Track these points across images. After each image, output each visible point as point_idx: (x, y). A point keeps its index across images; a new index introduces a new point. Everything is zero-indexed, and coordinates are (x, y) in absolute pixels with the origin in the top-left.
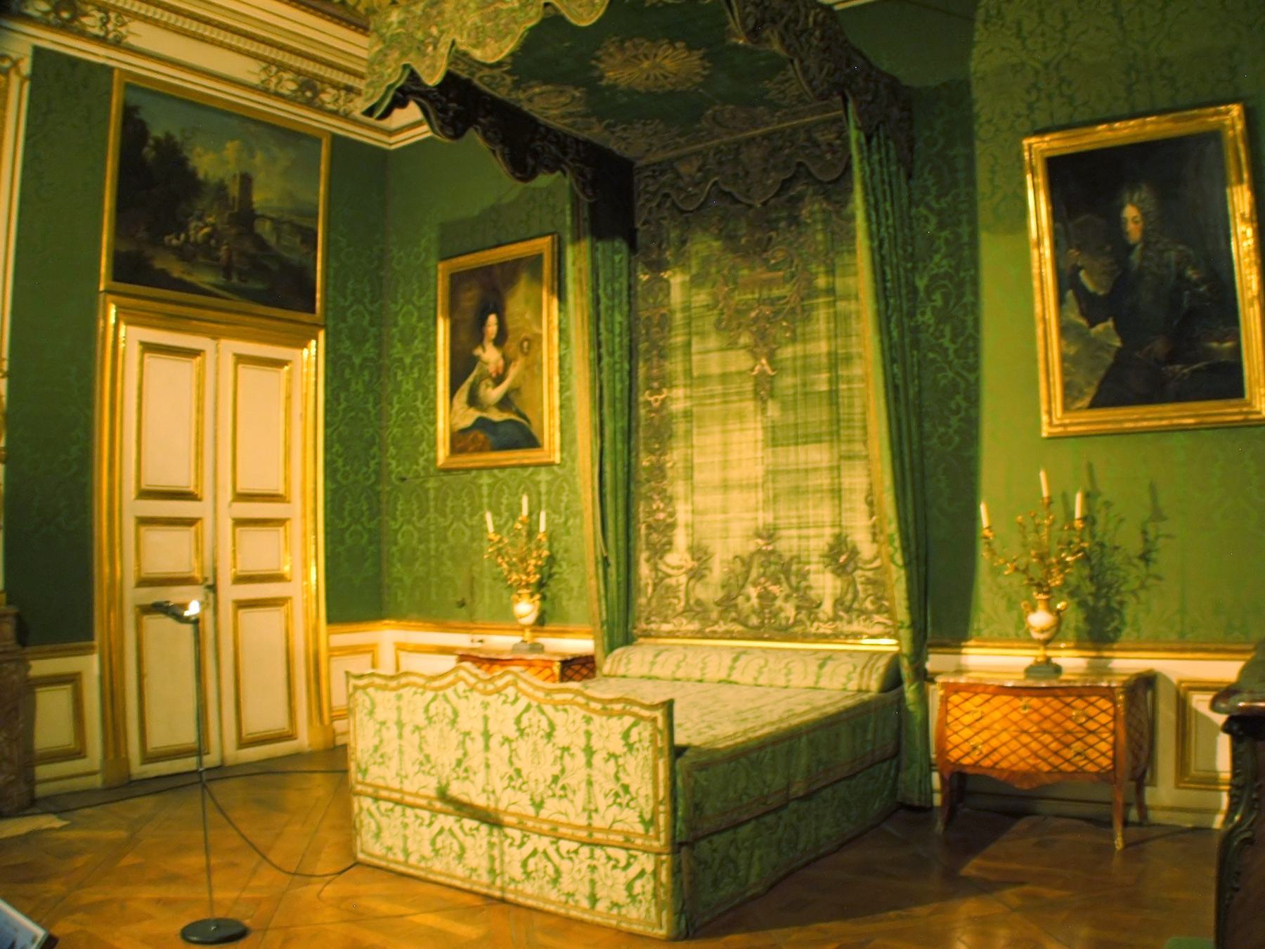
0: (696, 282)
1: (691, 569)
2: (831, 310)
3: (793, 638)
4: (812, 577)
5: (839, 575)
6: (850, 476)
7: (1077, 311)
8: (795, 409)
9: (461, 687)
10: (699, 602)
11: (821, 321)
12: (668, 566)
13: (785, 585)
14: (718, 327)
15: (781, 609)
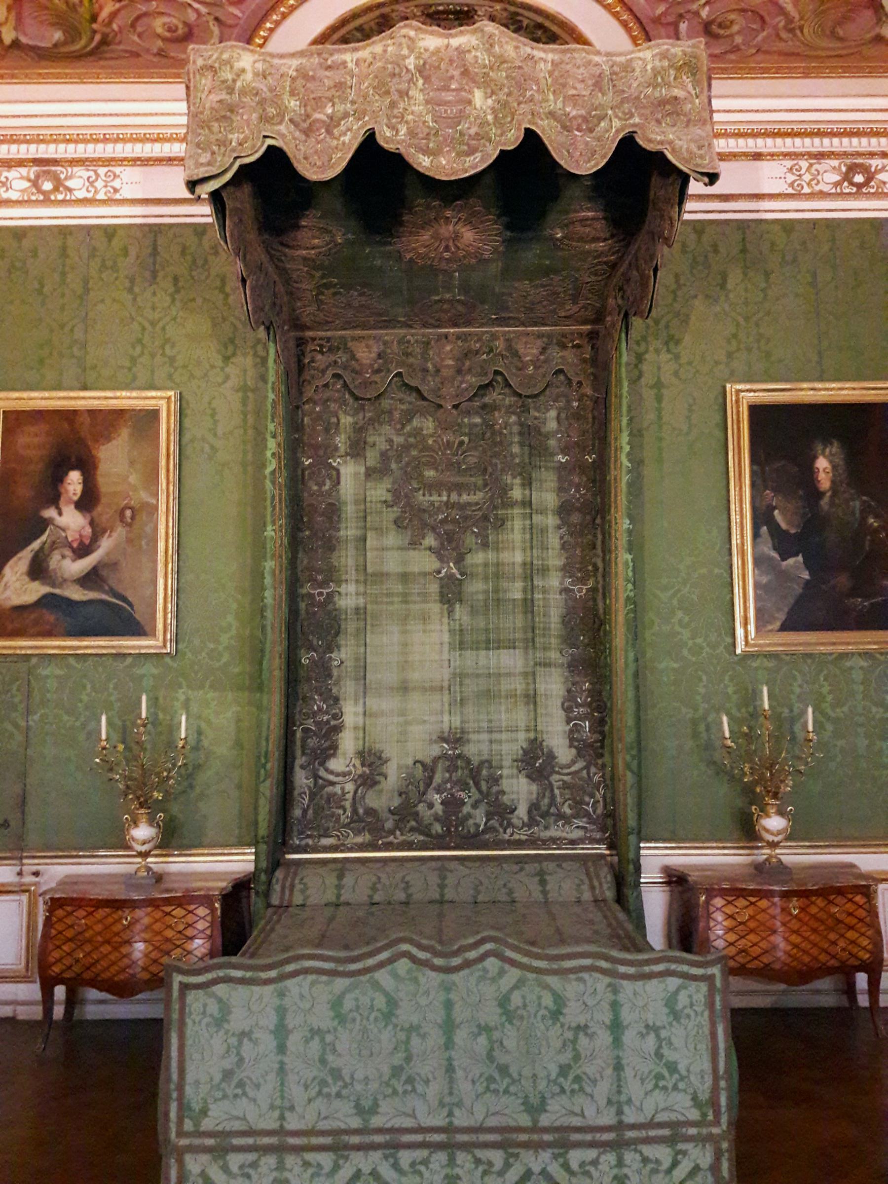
1: (360, 776)
5: (533, 780)
7: (770, 545)
8: (486, 613)
9: (403, 965)
10: (371, 812)
13: (473, 790)
15: (469, 816)
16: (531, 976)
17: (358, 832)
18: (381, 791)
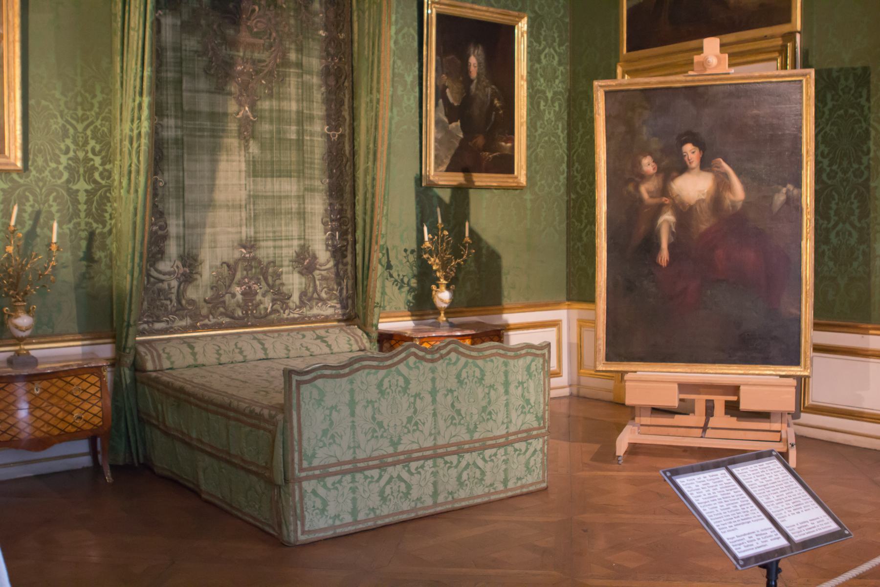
0: (187, 28)
1: (182, 274)
2: (300, 80)
3: (271, 324)
4: (284, 276)
6: (312, 204)
7: (443, 113)
8: (271, 150)
9: (412, 359)
10: (192, 302)
11: (292, 86)
12: (160, 272)
13: (263, 283)
14: (207, 71)
15: (261, 302)
16: (470, 361)
17: (182, 318)
18: (198, 286)
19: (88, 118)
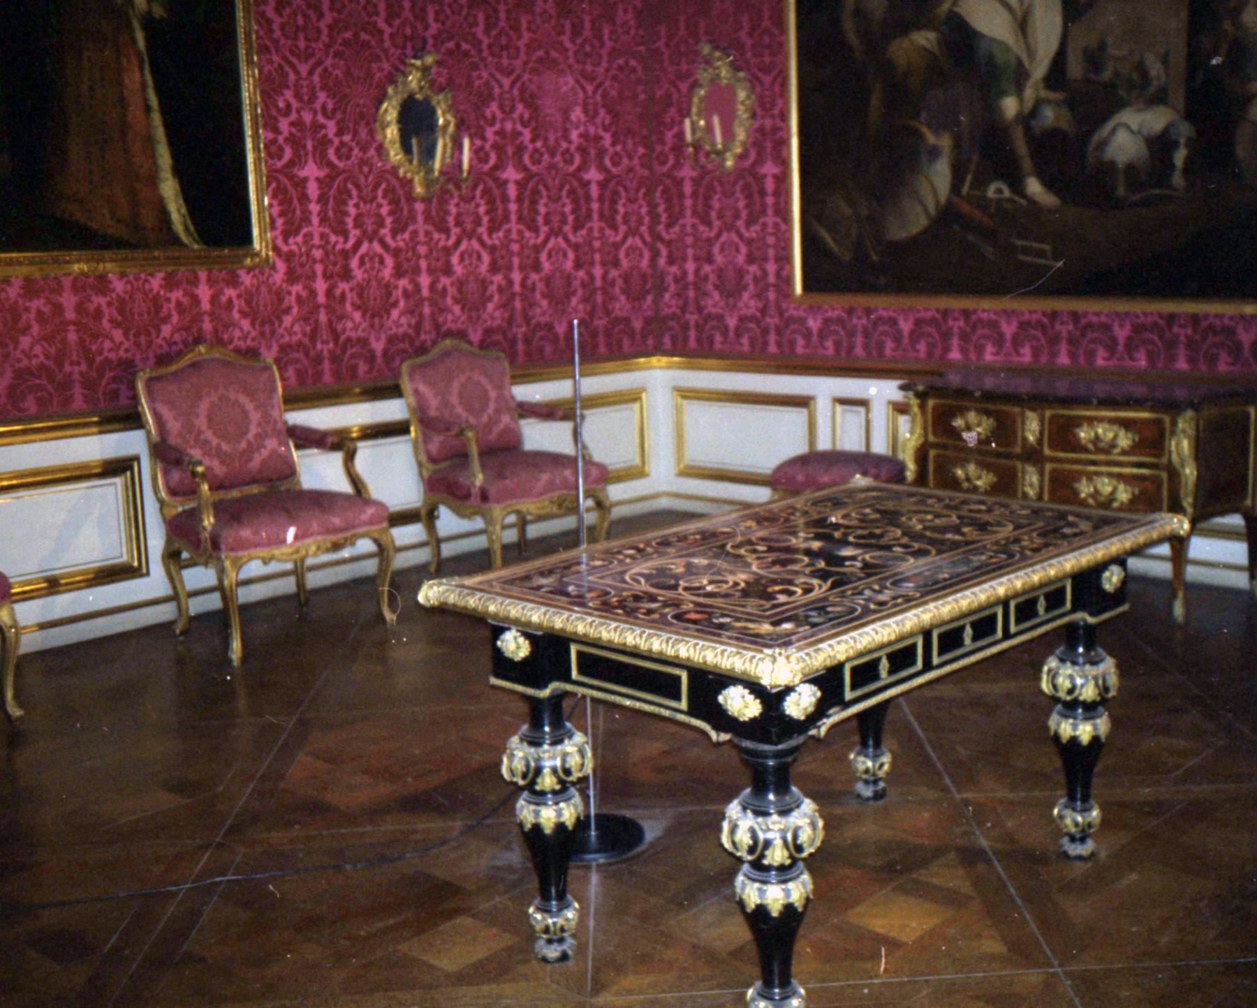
19: (313, 54)
